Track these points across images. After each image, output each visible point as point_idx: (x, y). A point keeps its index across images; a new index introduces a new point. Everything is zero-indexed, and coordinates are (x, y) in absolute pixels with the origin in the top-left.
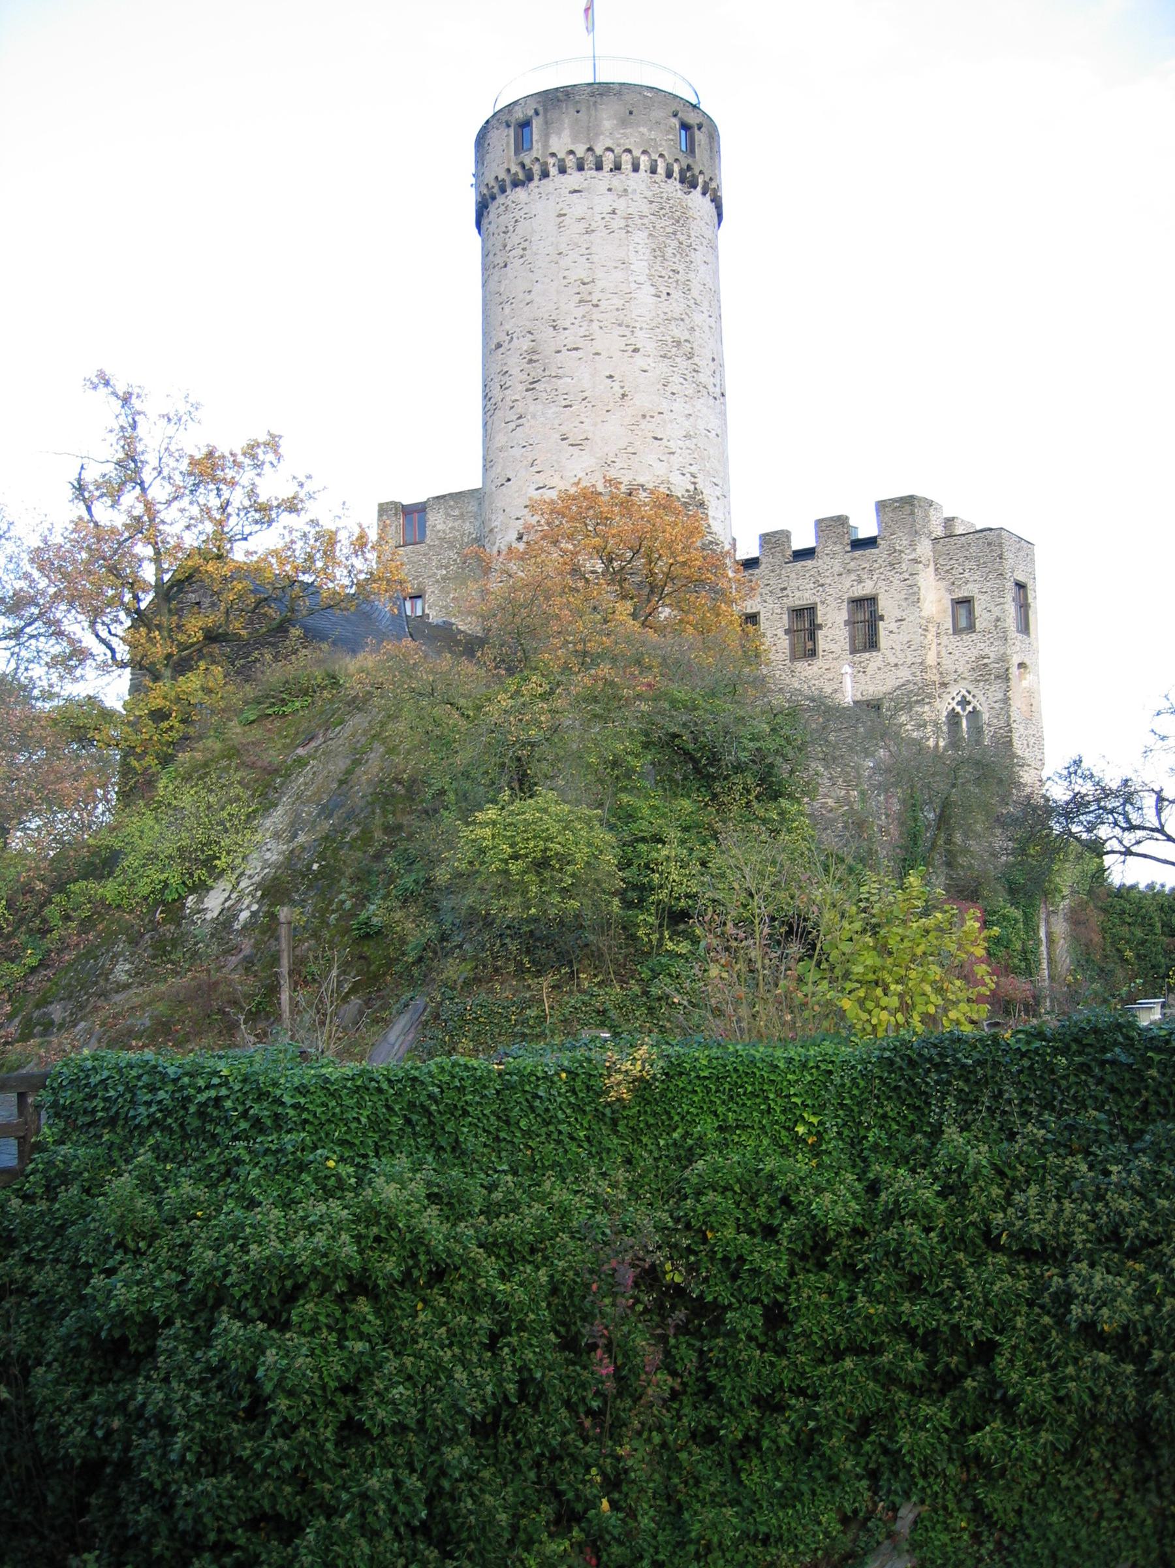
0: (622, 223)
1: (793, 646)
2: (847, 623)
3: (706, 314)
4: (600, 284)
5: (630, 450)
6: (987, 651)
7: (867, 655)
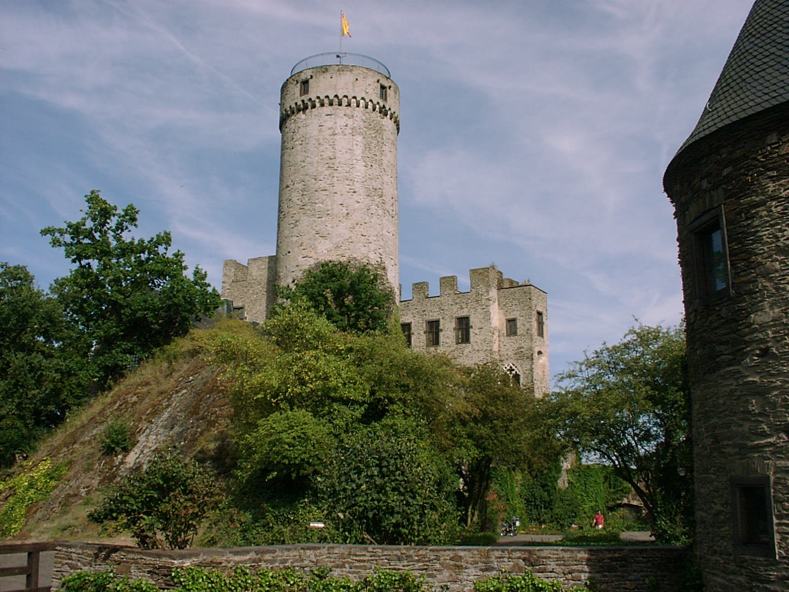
0: (350, 131)
1: (428, 339)
2: (454, 329)
3: (390, 176)
4: (338, 160)
5: (350, 240)
6: (523, 345)
7: (464, 345)
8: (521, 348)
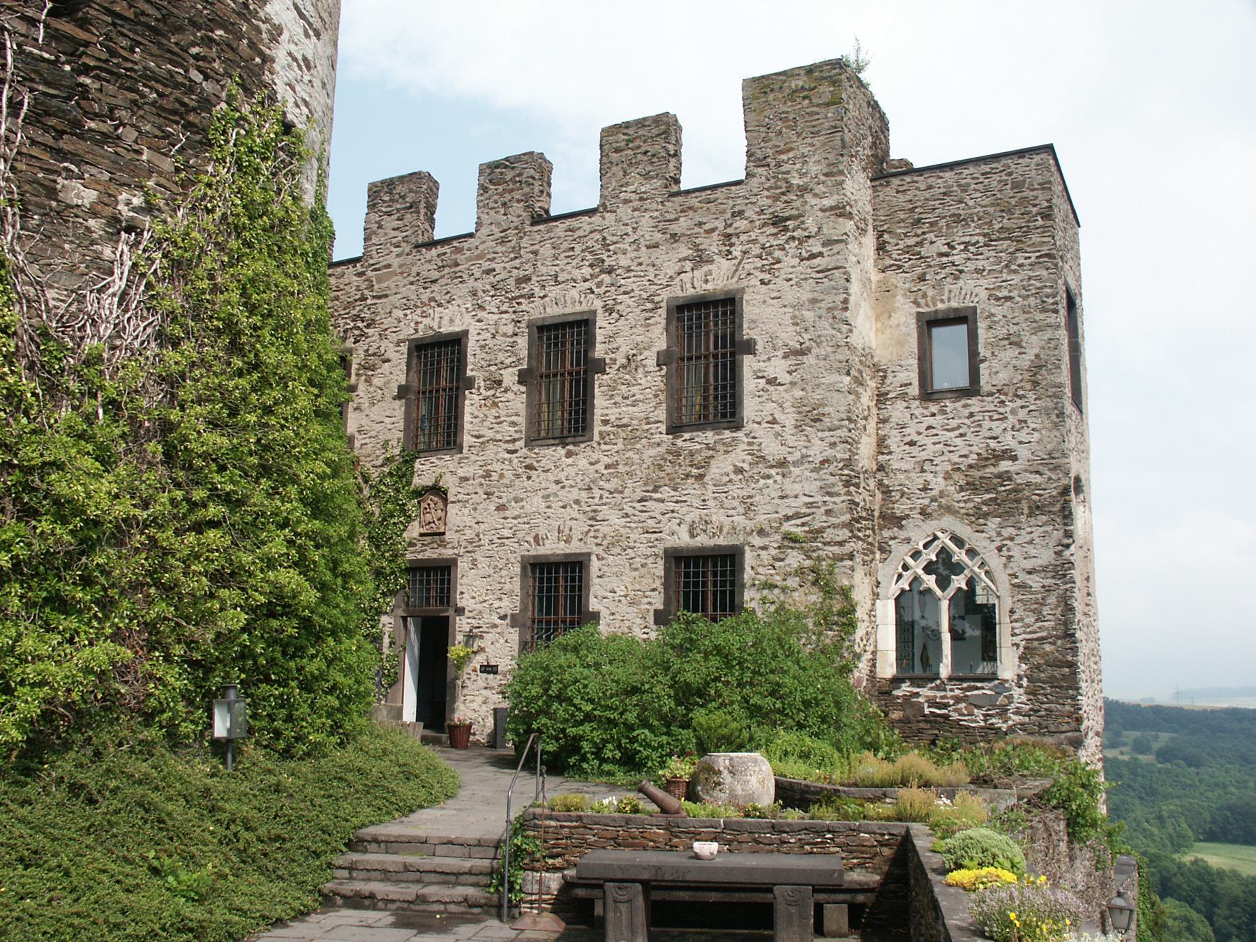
6: (1009, 441)
7: (709, 436)
8: (999, 456)
